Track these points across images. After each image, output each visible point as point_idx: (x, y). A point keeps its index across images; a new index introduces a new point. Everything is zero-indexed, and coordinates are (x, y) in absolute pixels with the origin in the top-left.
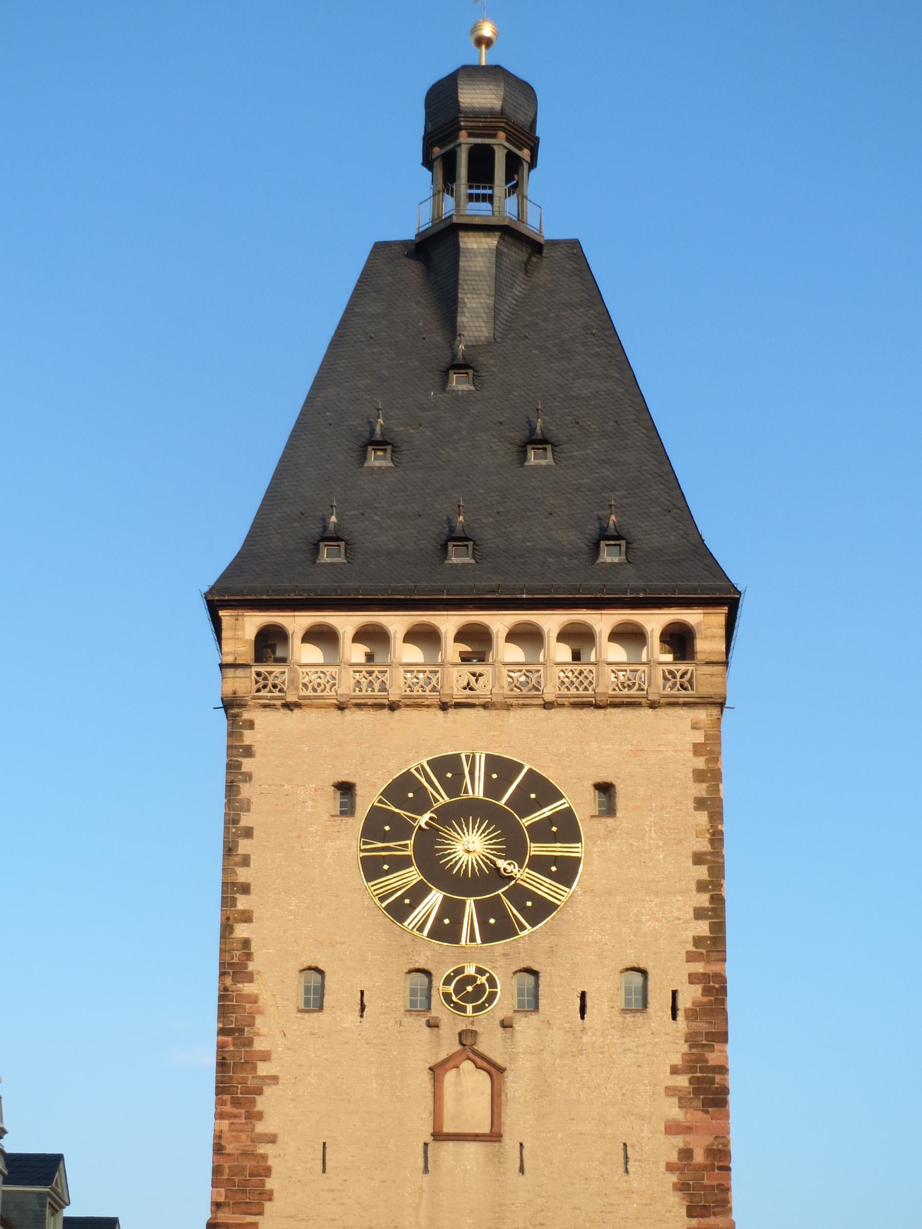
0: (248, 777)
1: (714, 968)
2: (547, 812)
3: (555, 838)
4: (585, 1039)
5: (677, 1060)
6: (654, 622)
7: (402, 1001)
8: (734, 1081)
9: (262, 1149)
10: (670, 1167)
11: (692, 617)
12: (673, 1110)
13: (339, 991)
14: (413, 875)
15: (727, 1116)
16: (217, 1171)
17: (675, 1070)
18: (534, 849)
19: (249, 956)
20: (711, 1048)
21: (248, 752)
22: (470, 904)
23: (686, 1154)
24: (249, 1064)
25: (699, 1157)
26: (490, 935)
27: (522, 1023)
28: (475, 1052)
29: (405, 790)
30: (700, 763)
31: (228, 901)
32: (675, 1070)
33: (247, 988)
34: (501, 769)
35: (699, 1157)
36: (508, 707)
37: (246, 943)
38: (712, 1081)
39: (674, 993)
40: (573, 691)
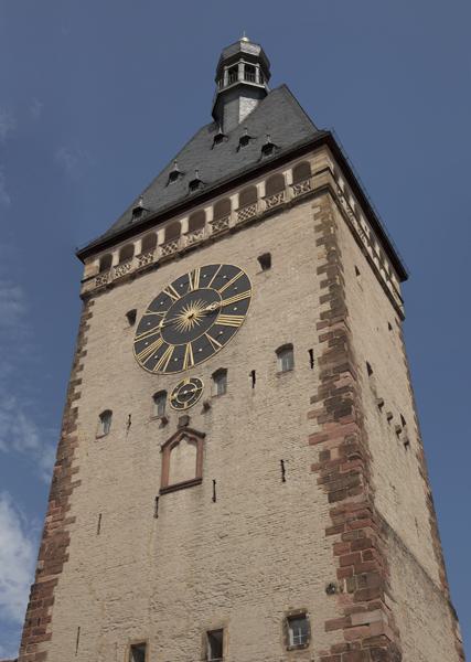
2: (232, 281)
3: (236, 292)
4: (255, 399)
5: (315, 392)
10: (314, 469)
12: (314, 427)
13: (118, 420)
14: (160, 341)
16: (42, 549)
17: (314, 400)
19: (76, 416)
23: (325, 455)
24: (69, 477)
25: (335, 455)
26: (199, 357)
27: (217, 407)
28: (188, 430)
32: (314, 400)
34: (208, 271)
35: (335, 455)
39: (311, 352)
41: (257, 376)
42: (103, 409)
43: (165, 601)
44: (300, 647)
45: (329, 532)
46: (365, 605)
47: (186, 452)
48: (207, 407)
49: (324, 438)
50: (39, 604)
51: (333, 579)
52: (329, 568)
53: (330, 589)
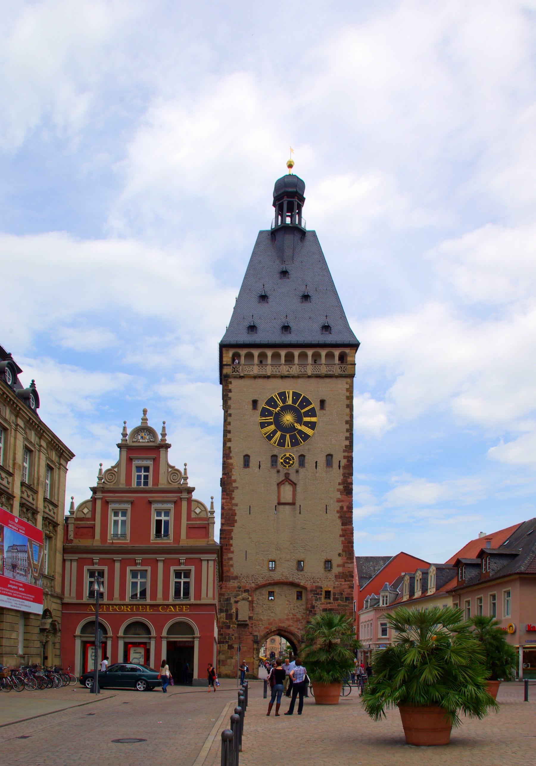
0: (230, 398)
1: (350, 454)
3: (310, 416)
4: (317, 475)
5: (340, 481)
6: (337, 352)
7: (269, 464)
8: (355, 487)
9: (234, 508)
10: (338, 512)
11: (347, 350)
12: (338, 495)
13: (253, 462)
14: (272, 427)
15: (352, 497)
17: (339, 484)
18: (306, 419)
19: (230, 452)
20: (348, 478)
21: (230, 391)
22: (288, 436)
23: (342, 508)
24: (231, 484)
25: (345, 509)
27: (301, 470)
29: (271, 402)
30: (348, 394)
31: (225, 436)
32: (339, 484)
33: (230, 461)
34: (296, 395)
35: (345, 509)
36: (298, 377)
37: (230, 448)
38: (349, 487)
39: (340, 461)
40: (315, 373)
41: (318, 465)
42: (245, 453)
43: (282, 547)
44: (329, 571)
45: (341, 536)
46: (349, 561)
47: (287, 490)
48: (297, 471)
49: (342, 501)
50: (225, 538)
51: (341, 552)
52: (339, 548)
53: (339, 555)
